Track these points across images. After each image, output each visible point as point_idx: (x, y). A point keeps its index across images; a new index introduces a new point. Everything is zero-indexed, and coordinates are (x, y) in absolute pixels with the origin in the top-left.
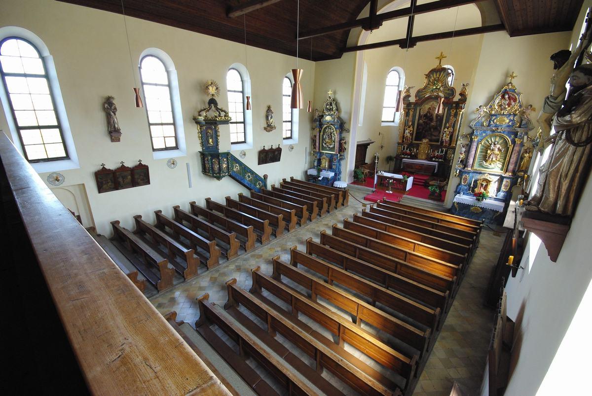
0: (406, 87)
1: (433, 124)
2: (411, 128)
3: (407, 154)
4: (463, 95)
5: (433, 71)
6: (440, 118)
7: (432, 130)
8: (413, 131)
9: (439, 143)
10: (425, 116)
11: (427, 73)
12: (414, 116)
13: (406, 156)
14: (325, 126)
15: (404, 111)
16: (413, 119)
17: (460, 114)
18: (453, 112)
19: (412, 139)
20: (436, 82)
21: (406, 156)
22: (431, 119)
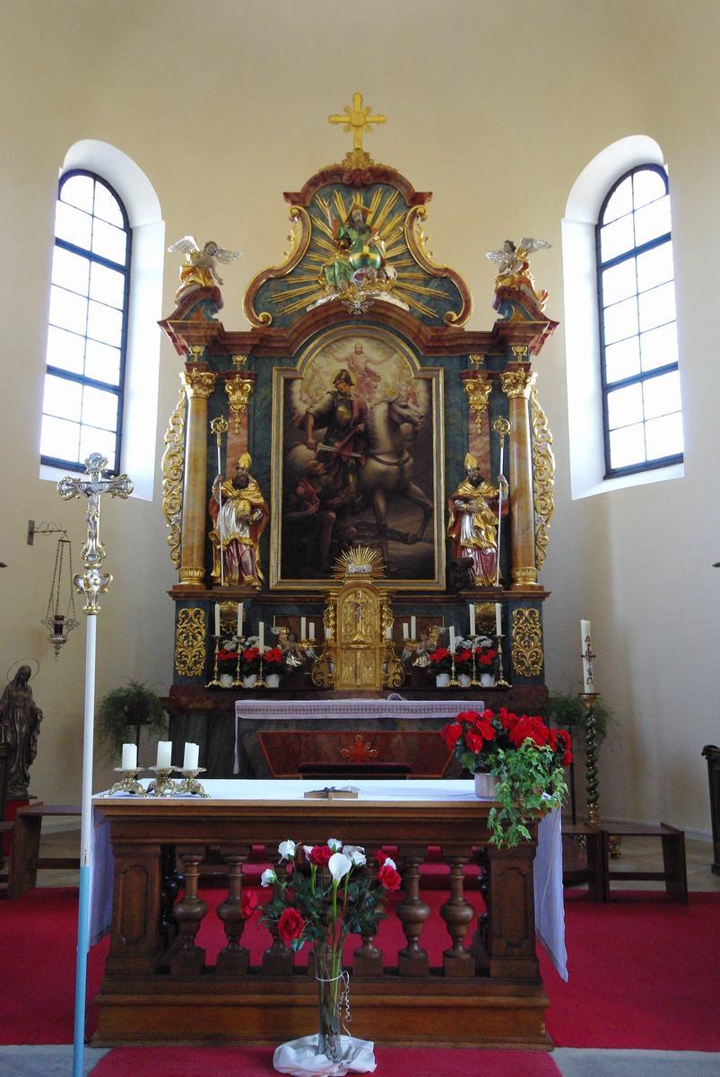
0: (186, 247)
1: (375, 465)
2: (252, 493)
3: (253, 663)
4: (513, 296)
5: (328, 180)
6: (415, 433)
7: (381, 504)
8: (266, 509)
9: (440, 581)
10: (326, 417)
11: (297, 187)
13: (250, 682)
16: (251, 436)
17: (520, 398)
19: (265, 565)
20: (354, 235)
21: (250, 682)
22: (365, 441)
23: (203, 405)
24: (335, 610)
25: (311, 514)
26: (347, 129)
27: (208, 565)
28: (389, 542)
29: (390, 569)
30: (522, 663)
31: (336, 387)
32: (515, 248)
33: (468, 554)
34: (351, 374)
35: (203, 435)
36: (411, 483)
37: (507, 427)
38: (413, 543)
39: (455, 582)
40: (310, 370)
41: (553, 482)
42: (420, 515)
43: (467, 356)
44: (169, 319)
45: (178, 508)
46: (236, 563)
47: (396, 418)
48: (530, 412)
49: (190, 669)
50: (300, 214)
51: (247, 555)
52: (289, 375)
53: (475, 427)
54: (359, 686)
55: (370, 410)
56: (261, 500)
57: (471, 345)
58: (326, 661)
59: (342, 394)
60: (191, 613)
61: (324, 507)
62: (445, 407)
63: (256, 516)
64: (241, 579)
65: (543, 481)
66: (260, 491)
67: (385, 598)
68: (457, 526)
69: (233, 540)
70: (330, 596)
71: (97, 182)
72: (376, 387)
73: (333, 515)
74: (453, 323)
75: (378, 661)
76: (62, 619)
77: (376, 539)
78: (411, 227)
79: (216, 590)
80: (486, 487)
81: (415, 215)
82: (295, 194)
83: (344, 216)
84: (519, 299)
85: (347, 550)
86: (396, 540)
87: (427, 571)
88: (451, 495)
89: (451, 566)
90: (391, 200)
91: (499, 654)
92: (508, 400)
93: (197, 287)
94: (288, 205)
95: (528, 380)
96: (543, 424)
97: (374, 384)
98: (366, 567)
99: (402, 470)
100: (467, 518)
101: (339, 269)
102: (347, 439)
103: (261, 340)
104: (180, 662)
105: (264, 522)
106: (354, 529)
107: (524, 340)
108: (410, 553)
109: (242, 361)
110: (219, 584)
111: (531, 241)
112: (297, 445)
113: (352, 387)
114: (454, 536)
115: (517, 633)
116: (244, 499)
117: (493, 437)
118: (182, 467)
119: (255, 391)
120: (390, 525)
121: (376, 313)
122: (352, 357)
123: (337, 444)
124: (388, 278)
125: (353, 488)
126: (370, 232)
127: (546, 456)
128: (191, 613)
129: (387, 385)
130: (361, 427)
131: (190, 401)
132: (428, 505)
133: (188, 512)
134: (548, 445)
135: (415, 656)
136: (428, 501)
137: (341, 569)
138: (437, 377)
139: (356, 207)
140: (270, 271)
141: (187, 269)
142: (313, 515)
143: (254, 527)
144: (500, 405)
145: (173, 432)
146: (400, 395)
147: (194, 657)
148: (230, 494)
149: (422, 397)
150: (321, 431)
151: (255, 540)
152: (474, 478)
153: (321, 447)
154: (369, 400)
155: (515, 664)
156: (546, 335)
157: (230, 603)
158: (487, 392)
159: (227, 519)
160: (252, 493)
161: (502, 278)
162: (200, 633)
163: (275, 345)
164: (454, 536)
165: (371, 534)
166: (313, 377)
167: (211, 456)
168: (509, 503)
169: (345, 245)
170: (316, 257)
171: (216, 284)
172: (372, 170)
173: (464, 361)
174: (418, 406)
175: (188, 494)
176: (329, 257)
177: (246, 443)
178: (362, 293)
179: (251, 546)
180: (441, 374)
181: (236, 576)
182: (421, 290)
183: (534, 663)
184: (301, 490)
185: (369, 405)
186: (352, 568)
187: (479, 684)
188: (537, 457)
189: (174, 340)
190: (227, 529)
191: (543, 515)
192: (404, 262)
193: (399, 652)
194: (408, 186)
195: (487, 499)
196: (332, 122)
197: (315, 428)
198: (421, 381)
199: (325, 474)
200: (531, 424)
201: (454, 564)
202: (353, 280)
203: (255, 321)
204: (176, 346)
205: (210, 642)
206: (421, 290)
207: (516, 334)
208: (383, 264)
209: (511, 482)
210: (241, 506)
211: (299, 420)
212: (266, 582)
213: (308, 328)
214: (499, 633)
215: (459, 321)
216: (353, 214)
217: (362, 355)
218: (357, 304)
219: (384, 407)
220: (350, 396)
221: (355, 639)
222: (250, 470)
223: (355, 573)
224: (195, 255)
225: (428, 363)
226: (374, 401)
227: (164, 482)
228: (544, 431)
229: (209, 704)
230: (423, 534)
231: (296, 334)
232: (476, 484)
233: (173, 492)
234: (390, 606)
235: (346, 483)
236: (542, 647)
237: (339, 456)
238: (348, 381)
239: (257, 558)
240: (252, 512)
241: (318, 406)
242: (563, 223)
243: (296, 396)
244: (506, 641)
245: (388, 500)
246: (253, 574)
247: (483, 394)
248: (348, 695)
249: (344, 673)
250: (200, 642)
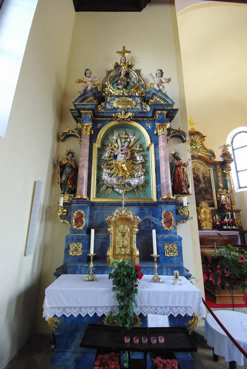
4: (226, 155)
6: (208, 180)
14: (113, 123)
38: (210, 200)
42: (211, 195)
47: (204, 177)
88: (217, 192)
99: (206, 187)
120: (205, 197)
125: (197, 189)
129: (202, 170)
130: (198, 178)
135: (216, 222)
144: (224, 175)
149: (208, 173)
161: (223, 151)
182: (206, 153)
183: (240, 224)
185: (199, 174)
206: (206, 153)
215: (214, 159)
238: (194, 170)
245: (204, 192)
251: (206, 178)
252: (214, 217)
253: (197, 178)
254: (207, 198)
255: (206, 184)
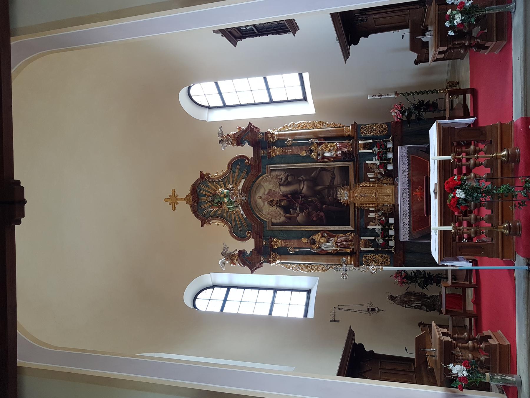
0: (224, 263)
1: (304, 190)
2: (317, 237)
5: (196, 211)
6: (292, 175)
7: (320, 187)
8: (323, 232)
9: (350, 164)
10: (286, 210)
12: (287, 236)
15: (274, 261)
16: (294, 238)
17: (278, 135)
18: (278, 150)
20: (217, 200)
22: (295, 194)
23: (282, 256)
24: (363, 204)
25: (324, 215)
26: (177, 204)
27: (345, 254)
28: (334, 184)
29: (345, 184)
30: (382, 131)
31: (274, 206)
32: (222, 139)
33: (339, 153)
34: (269, 200)
35: (294, 256)
36: (311, 176)
37: (290, 140)
38: (335, 175)
39: (350, 158)
40: (268, 216)
41: (310, 122)
42: (324, 172)
43: (262, 156)
44: (251, 270)
45: (323, 266)
46: (345, 243)
47: (286, 183)
48: (283, 131)
49: (387, 260)
50: (209, 221)
51: (342, 239)
52: (270, 224)
53: (289, 152)
54: (393, 195)
55: (283, 193)
56: (320, 233)
57: (258, 155)
58: (382, 208)
59: (277, 204)
60: (364, 260)
61: (321, 210)
62: (282, 164)
63: (326, 235)
64: (351, 241)
65: (309, 125)
66: (316, 234)
67: (358, 185)
68: (328, 158)
69: (336, 244)
70: (357, 206)
71: (197, 298)
72: (274, 191)
73: (324, 206)
74: (249, 162)
75: (382, 187)
76: (369, 308)
77: (333, 189)
78: (213, 179)
79: (355, 251)
80: (313, 147)
81: (208, 178)
82: (201, 223)
83: (209, 204)
84: (240, 137)
85: (339, 200)
86: (334, 181)
87: (347, 169)
88: (316, 161)
89: (344, 160)
90: (203, 187)
91: (379, 141)
92: (278, 139)
93: (239, 259)
94: (205, 225)
95: (271, 133)
96: (287, 126)
97: (273, 191)
98: (346, 193)
99: (306, 180)
100: (325, 154)
101: (230, 205)
102: (294, 201)
103: (257, 235)
104: (385, 264)
105: (328, 232)
106: (330, 198)
107: (257, 135)
108: (339, 176)
109: (265, 242)
110: (353, 249)
111: (219, 134)
112: (297, 220)
113: (274, 200)
114: (332, 159)
115: (371, 134)
116: (320, 240)
117: (293, 145)
118: (307, 265)
119: (276, 237)
121: (246, 192)
122: (263, 200)
123: (296, 205)
124: (233, 187)
125: (314, 199)
126: (215, 194)
127: (300, 124)
128: (364, 260)
129: (273, 186)
130: (289, 196)
131: (281, 262)
132: (320, 169)
133: (325, 262)
134: (295, 124)
136: (318, 169)
137: (346, 202)
138: (270, 167)
139: (207, 200)
140: (230, 232)
141: (232, 263)
142: (324, 214)
143: (330, 236)
144: (281, 142)
145: (293, 268)
146: (277, 181)
147: (382, 258)
148: (318, 245)
149: (277, 173)
150: (291, 211)
151: (336, 236)
152: (310, 152)
153: (298, 211)
154: (279, 193)
155: (383, 134)
156: (254, 126)
157: (360, 245)
158: (276, 148)
159: (328, 247)
160: (317, 237)
161: (233, 144)
162: (373, 256)
163: (259, 229)
164: (332, 159)
165: (332, 191)
166: (271, 215)
167: (302, 253)
168: (319, 138)
169: (221, 203)
170: (225, 215)
171: (237, 252)
172: (192, 195)
173: (263, 157)
174: (281, 174)
175: (318, 262)
176: (225, 209)
177: (297, 240)
178: (239, 197)
179: (338, 237)
180: (269, 166)
181: (350, 243)
183: (382, 127)
184: (315, 219)
186: (346, 198)
187: (391, 148)
188: (300, 128)
189: (258, 268)
190: (331, 246)
191: (323, 125)
192: (226, 181)
193: (378, 179)
194: (198, 180)
195: (318, 147)
196: (175, 209)
197: (291, 214)
198: (271, 173)
199: (308, 209)
200: (287, 131)
201: (343, 159)
202: (234, 200)
203: (250, 237)
204: (260, 267)
205: (376, 252)
207: (254, 138)
208: (228, 189)
209: (310, 138)
210: (323, 241)
211: (287, 220)
212: (352, 232)
213: (252, 216)
214: (371, 141)
215: (248, 160)
216: (209, 201)
217: (262, 196)
218: (243, 198)
219: (281, 187)
220: (278, 200)
221: (374, 196)
222: (308, 238)
223: (348, 197)
224: (227, 259)
225: (265, 171)
226: (280, 191)
227: (312, 271)
228: (290, 126)
229: (401, 252)
230: (331, 171)
231: (255, 221)
232: (312, 151)
233: (317, 268)
234: (360, 183)
235: (312, 201)
236: (375, 124)
237: (301, 204)
238: (272, 201)
239: (342, 235)
240: (325, 237)
241: (282, 213)
242: (208, 121)
243: (278, 221)
244: (374, 138)
245: (318, 185)
246: (349, 236)
247: (276, 149)
248: (397, 198)
249: (388, 200)
250: (377, 257)
251: (289, 179)
252: (371, 180)
253: (288, 198)
254: (330, 178)
255: (300, 181)
